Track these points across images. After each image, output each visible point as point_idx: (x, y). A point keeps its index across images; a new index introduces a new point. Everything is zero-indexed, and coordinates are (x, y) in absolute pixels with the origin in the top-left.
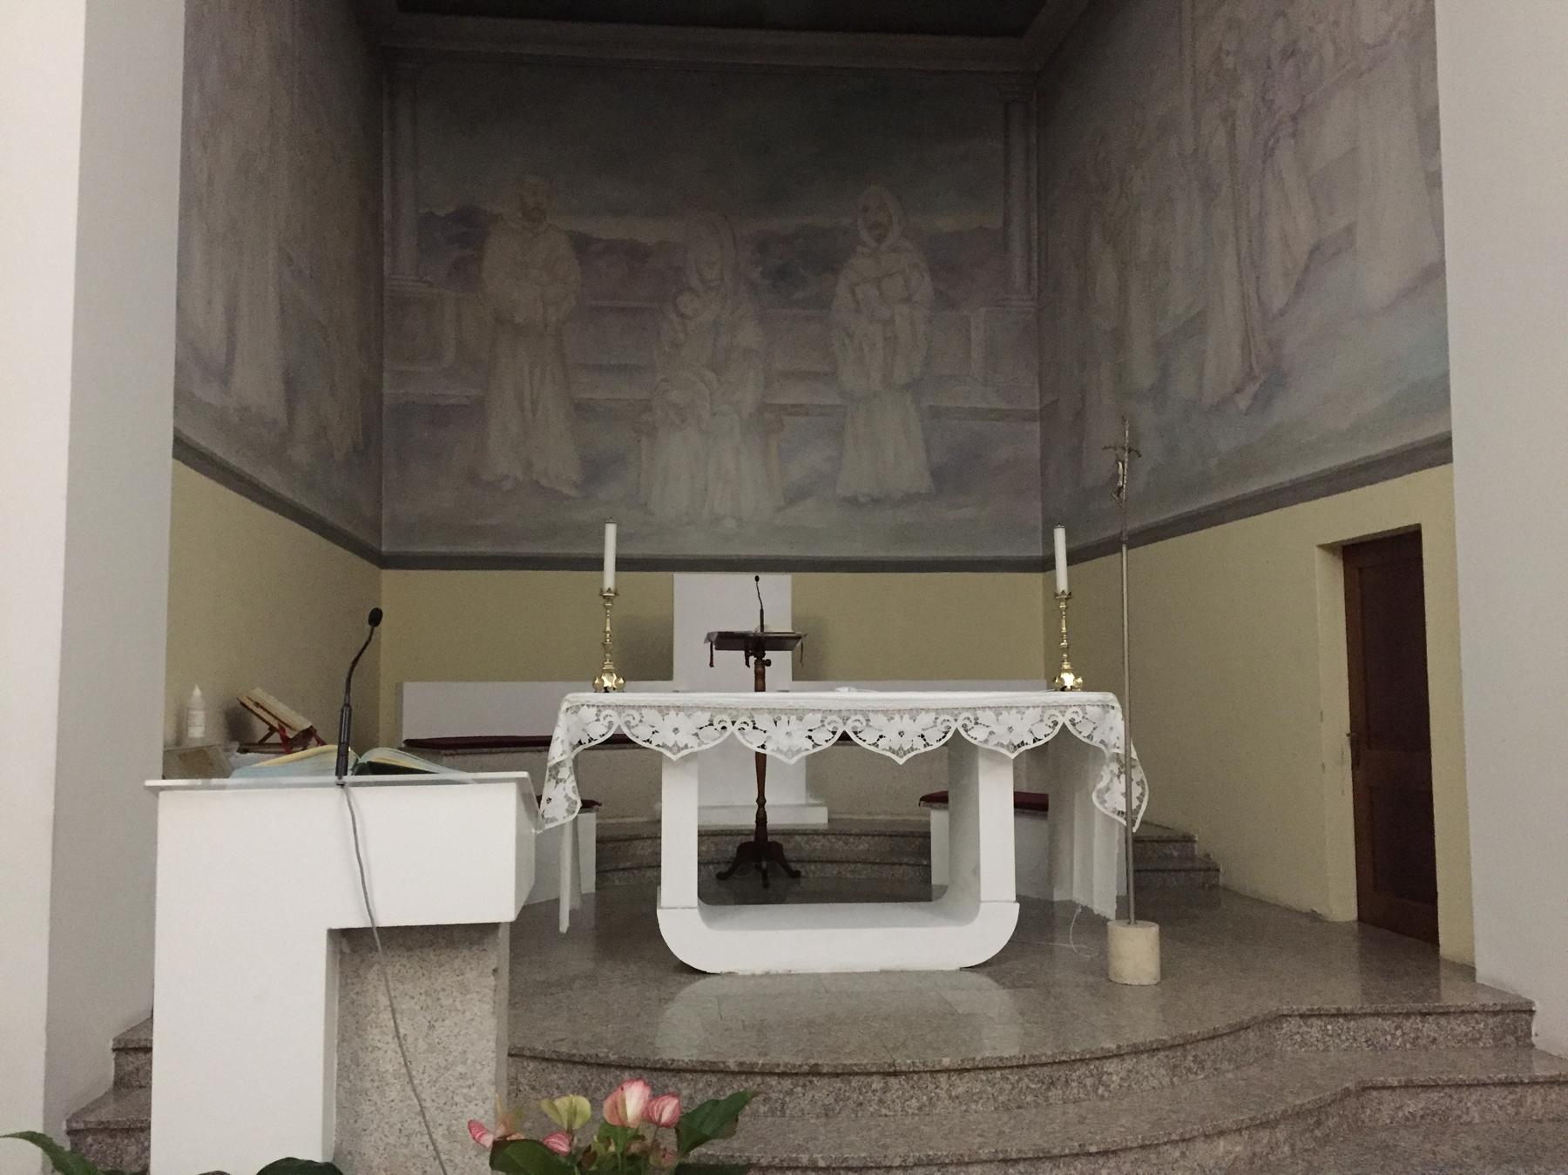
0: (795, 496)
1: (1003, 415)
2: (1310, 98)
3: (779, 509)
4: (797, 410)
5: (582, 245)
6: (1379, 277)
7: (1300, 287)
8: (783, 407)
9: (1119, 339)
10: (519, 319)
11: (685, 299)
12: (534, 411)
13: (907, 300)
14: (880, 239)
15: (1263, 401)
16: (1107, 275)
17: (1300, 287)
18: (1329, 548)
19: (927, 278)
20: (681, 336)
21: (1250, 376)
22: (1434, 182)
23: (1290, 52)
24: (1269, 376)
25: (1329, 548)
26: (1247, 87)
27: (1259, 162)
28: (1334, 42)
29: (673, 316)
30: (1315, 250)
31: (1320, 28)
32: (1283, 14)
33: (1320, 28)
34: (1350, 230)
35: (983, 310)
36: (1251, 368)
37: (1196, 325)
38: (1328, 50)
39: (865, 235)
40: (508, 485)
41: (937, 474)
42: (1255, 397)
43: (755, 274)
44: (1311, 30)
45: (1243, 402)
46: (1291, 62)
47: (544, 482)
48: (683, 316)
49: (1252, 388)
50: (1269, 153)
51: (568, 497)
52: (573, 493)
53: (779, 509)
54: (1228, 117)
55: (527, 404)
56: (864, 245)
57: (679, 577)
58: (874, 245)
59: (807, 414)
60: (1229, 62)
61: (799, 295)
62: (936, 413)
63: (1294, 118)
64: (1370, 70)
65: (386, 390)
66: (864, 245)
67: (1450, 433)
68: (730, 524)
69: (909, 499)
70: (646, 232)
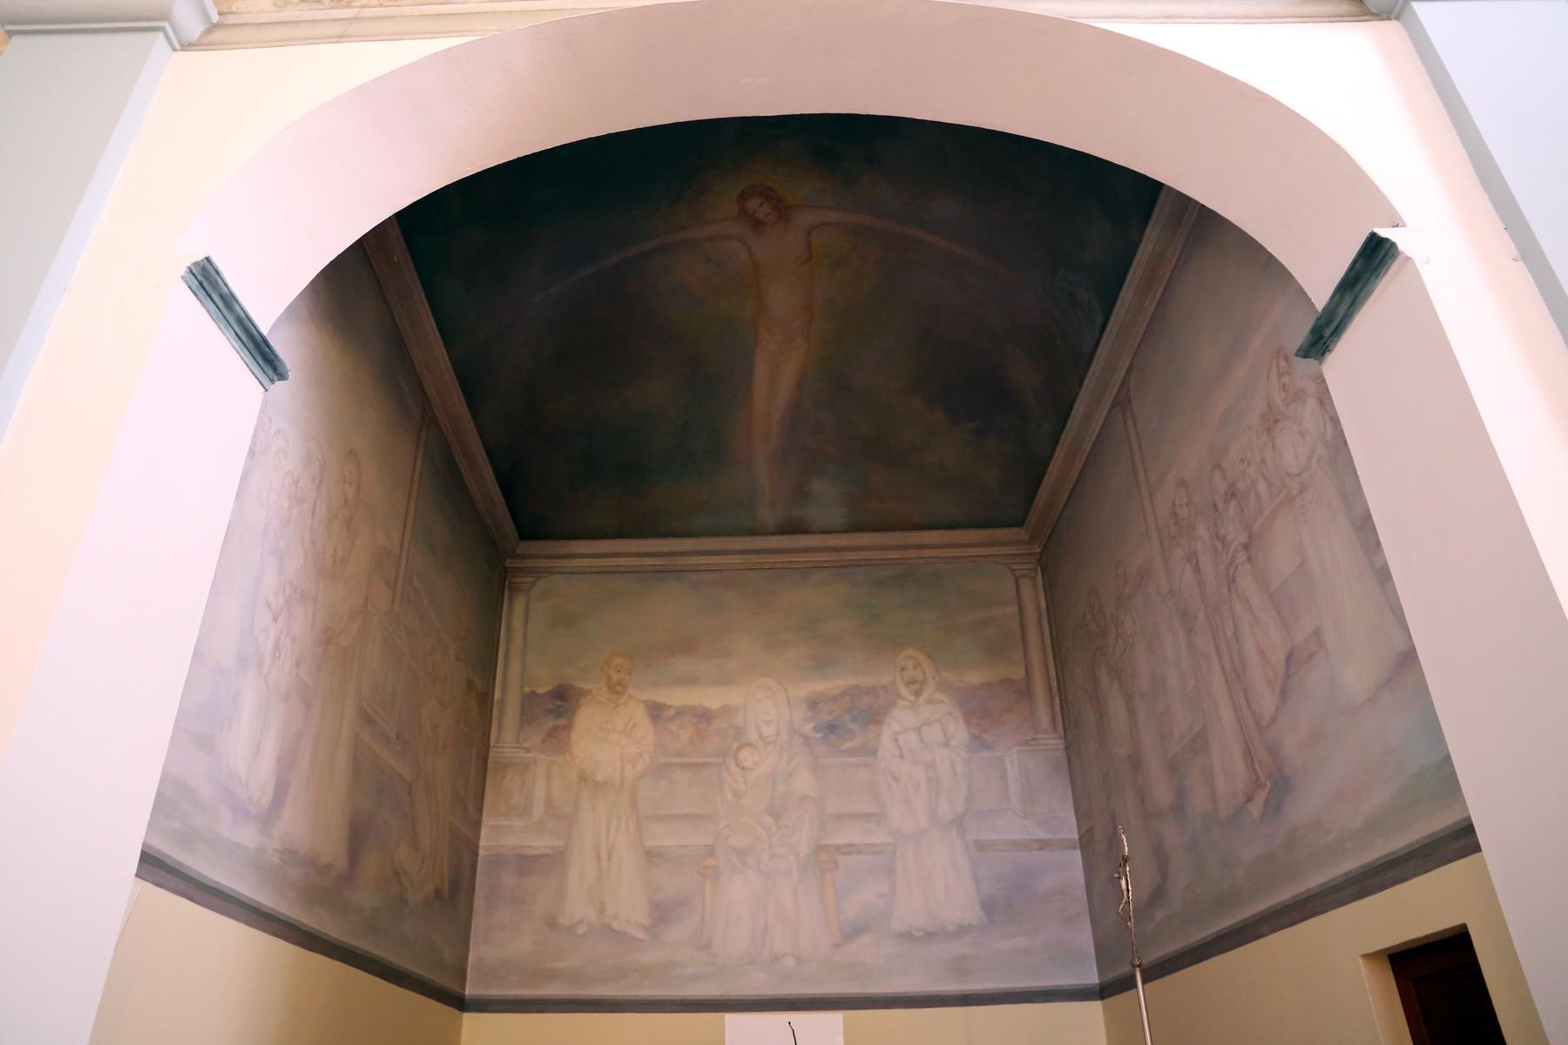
0: (852, 932)
1: (1043, 845)
2: (1255, 529)
3: (836, 946)
4: (848, 850)
5: (656, 712)
6: (1353, 671)
7: (1284, 693)
8: (838, 848)
9: (1136, 762)
10: (600, 777)
11: (745, 754)
12: (609, 860)
13: (947, 744)
14: (917, 694)
15: (1274, 807)
16: (1116, 706)
17: (1284, 693)
18: (1366, 956)
19: (962, 726)
20: (742, 787)
21: (1257, 784)
22: (1384, 576)
23: (1232, 494)
24: (1274, 783)
25: (1366, 956)
26: (1202, 531)
27: (1225, 590)
28: (1264, 477)
29: (735, 769)
30: (1289, 658)
31: (1251, 470)
32: (1218, 466)
33: (1251, 470)
34: (1317, 634)
35: (1015, 750)
36: (1258, 777)
37: (1199, 742)
38: (1262, 486)
39: (904, 691)
40: (581, 930)
41: (990, 907)
42: (1266, 803)
43: (808, 728)
44: (1243, 473)
45: (1256, 809)
46: (1233, 504)
47: (615, 925)
48: (743, 768)
49: (1261, 797)
50: (1232, 581)
51: (634, 939)
52: (641, 935)
53: (836, 946)
54: (1192, 558)
55: (604, 855)
56: (903, 698)
57: (729, 1018)
58: (912, 698)
59: (860, 853)
60: (1183, 512)
61: (848, 745)
62: (981, 846)
63: (1246, 547)
64: (1301, 491)
65: (482, 843)
66: (903, 698)
67: (1469, 818)
68: (790, 962)
69: (962, 930)
70: (711, 698)
